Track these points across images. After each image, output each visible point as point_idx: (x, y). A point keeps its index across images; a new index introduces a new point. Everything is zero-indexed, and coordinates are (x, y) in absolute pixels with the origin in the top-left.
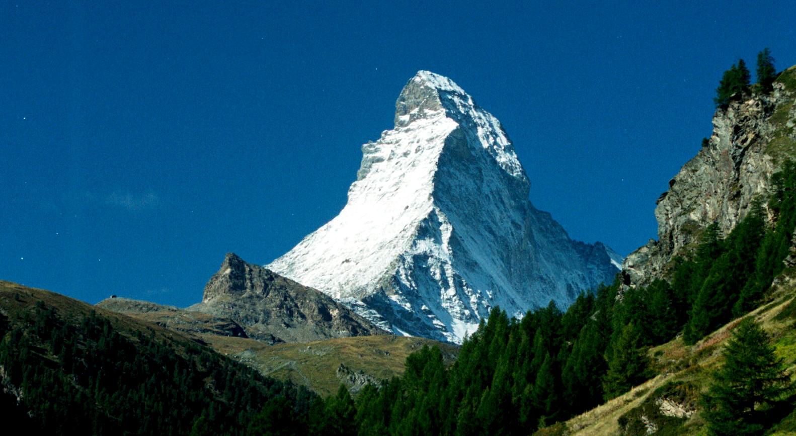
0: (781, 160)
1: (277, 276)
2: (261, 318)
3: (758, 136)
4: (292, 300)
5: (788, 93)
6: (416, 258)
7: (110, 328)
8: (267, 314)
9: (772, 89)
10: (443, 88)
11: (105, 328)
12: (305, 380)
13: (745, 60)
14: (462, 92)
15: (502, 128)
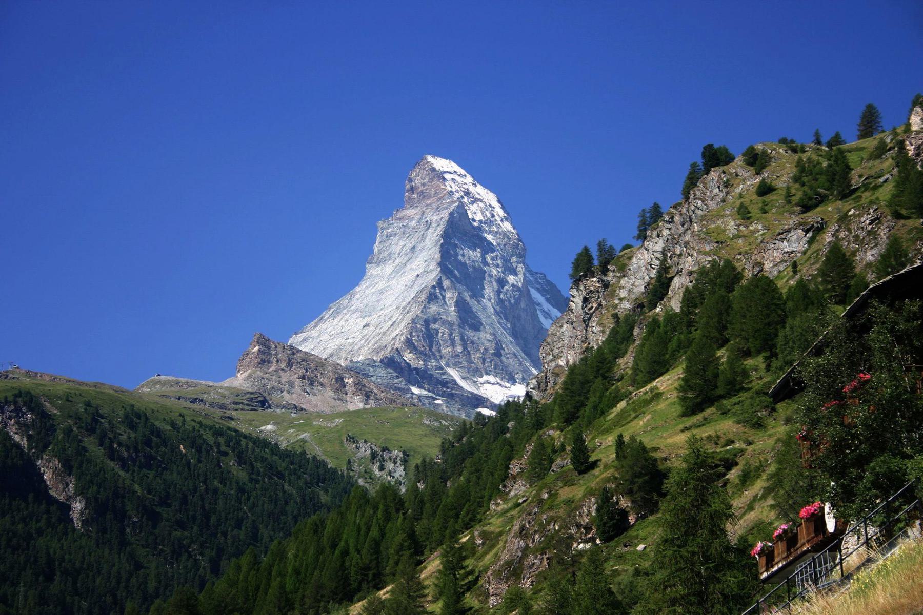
0: (608, 331)
1: (299, 351)
2: (286, 388)
3: (600, 305)
4: (312, 371)
5: (618, 275)
6: (427, 323)
7: (147, 419)
8: (291, 384)
9: (608, 270)
10: (445, 170)
11: (143, 419)
12: (316, 450)
13: (589, 247)
14: (463, 172)
15: (499, 201)
